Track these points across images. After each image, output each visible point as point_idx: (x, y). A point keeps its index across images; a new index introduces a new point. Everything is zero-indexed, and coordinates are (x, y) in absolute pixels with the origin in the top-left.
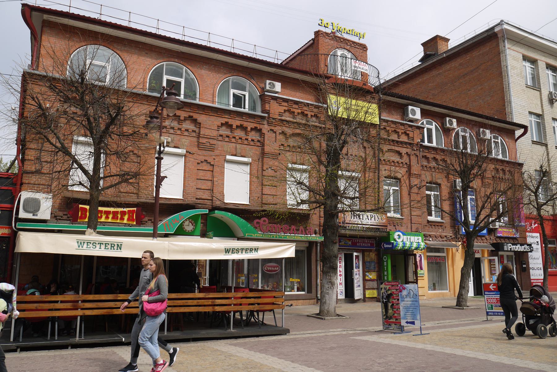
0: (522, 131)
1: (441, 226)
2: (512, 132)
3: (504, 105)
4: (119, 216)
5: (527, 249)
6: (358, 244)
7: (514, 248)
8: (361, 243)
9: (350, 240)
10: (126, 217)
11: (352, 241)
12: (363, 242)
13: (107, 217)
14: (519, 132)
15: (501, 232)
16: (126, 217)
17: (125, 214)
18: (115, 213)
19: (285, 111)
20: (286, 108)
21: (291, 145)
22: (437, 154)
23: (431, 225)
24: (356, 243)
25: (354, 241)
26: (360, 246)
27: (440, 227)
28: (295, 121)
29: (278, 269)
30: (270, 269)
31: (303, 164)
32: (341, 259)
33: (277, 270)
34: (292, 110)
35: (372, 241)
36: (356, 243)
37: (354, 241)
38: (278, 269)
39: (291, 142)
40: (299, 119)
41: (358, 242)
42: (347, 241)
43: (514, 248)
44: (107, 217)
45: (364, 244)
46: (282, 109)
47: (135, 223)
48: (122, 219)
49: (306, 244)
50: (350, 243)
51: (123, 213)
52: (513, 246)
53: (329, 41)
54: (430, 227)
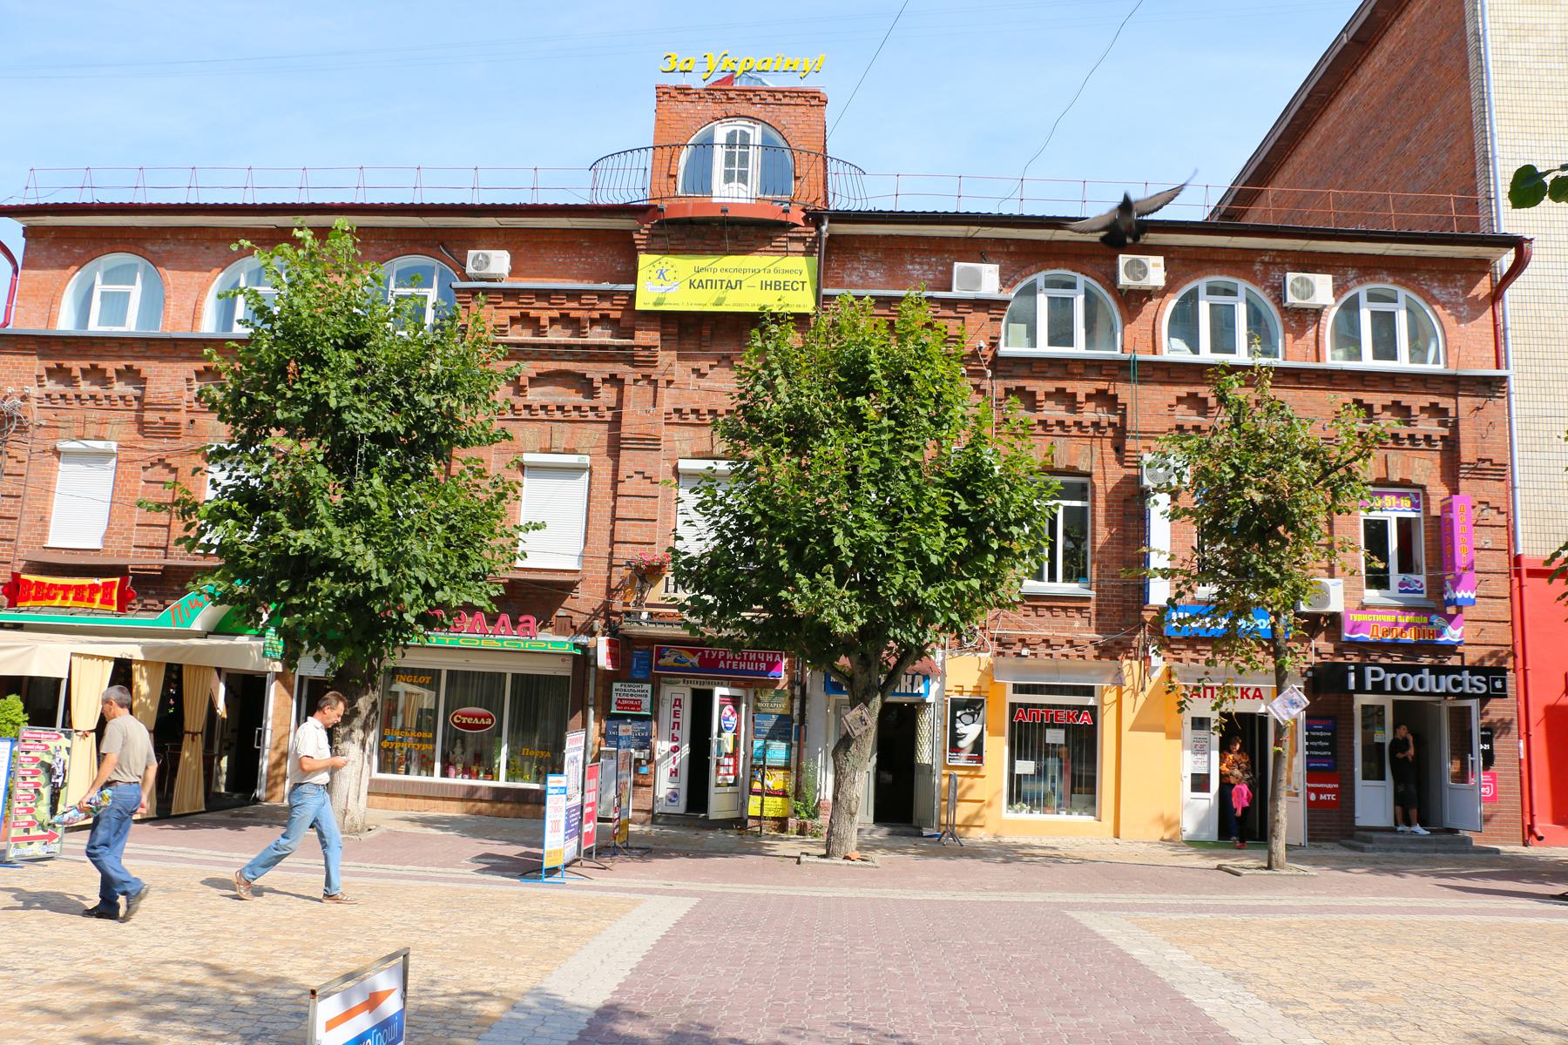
0: (1507, 259)
1: (1079, 610)
2: (1483, 266)
3: (1474, 175)
4: (86, 594)
5: (1472, 686)
6: (722, 665)
7: (1393, 680)
8: (734, 659)
9: (694, 653)
10: (98, 597)
11: (704, 654)
12: (742, 660)
13: (65, 598)
14: (1507, 259)
15: (1356, 627)
16: (71, 595)
17: (98, 591)
18: (80, 588)
19: (513, 320)
20: (517, 313)
21: (536, 405)
22: (1071, 376)
23: (1035, 608)
24: (717, 660)
25: (710, 654)
26: (730, 671)
27: (1077, 615)
28: (580, 341)
29: (489, 722)
30: (470, 720)
31: (573, 452)
32: (680, 706)
33: (488, 726)
34: (533, 313)
35: (774, 655)
36: (717, 660)
37: (710, 654)
38: (489, 722)
39: (535, 396)
40: (557, 336)
41: (724, 658)
42: (686, 655)
43: (1393, 680)
44: (65, 598)
45: (742, 665)
46: (503, 317)
47: (115, 608)
48: (91, 600)
49: (563, 660)
50: (695, 660)
51: (94, 588)
52: (1390, 676)
53: (689, 106)
54: (1033, 614)
